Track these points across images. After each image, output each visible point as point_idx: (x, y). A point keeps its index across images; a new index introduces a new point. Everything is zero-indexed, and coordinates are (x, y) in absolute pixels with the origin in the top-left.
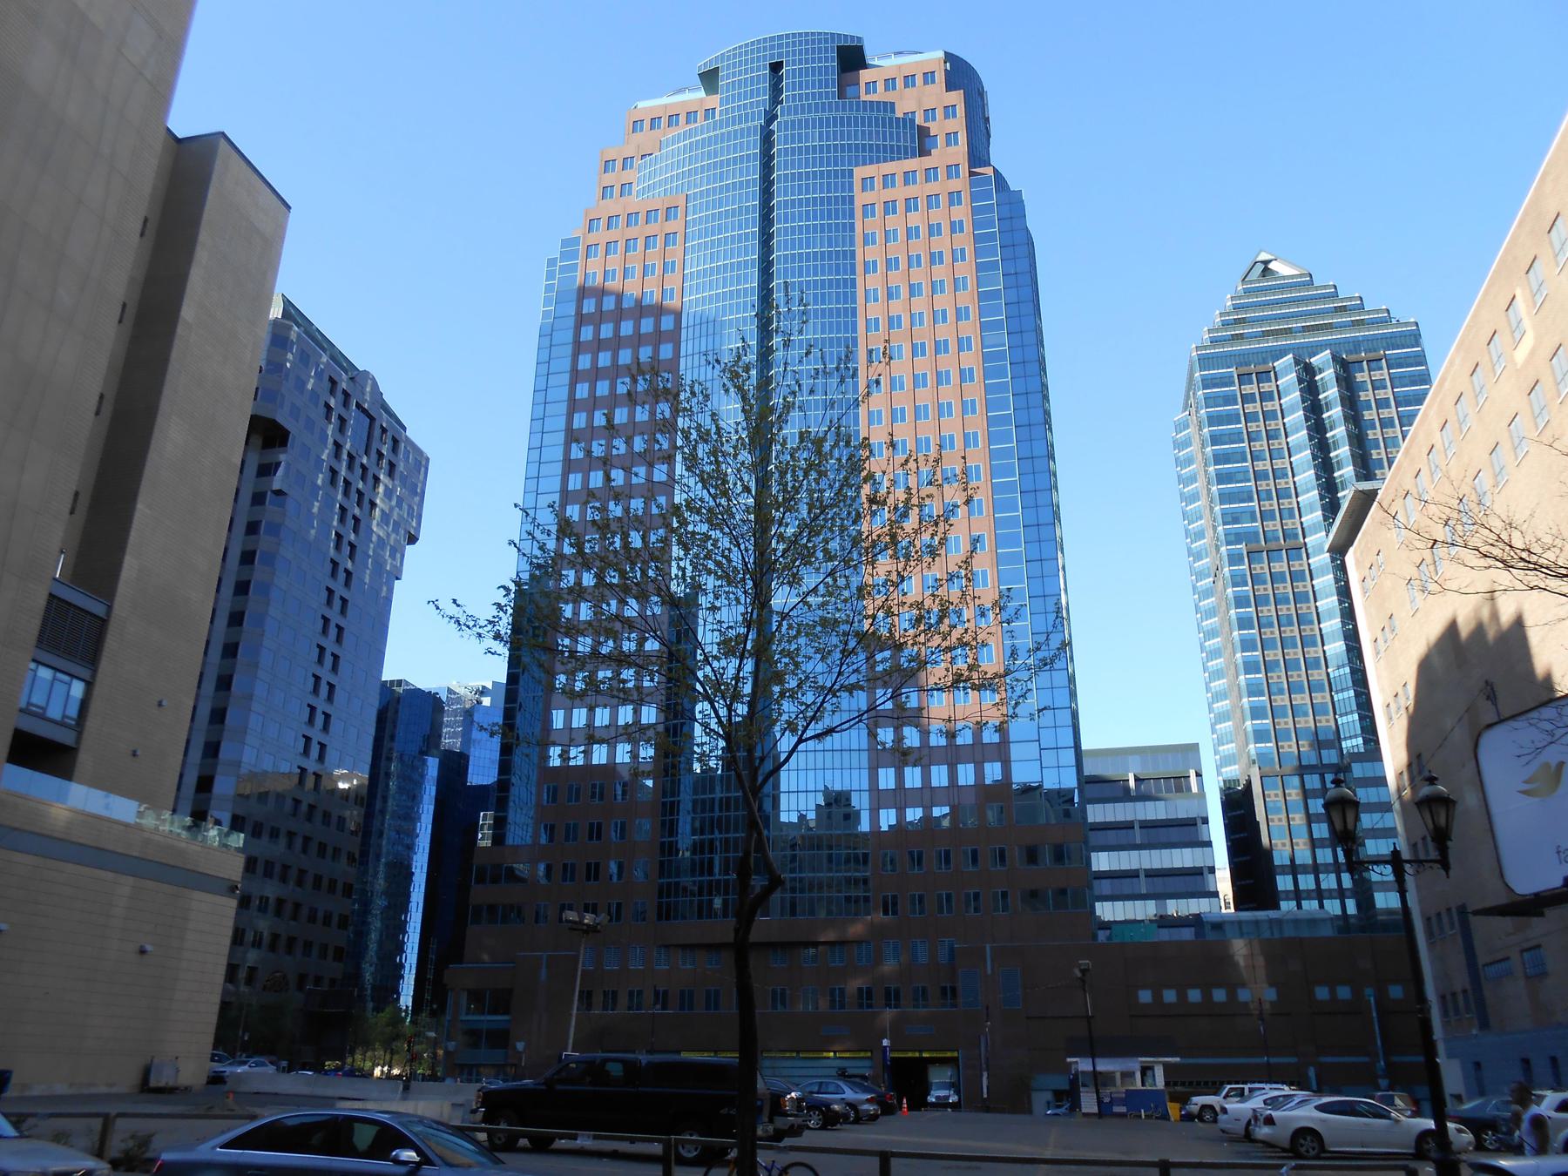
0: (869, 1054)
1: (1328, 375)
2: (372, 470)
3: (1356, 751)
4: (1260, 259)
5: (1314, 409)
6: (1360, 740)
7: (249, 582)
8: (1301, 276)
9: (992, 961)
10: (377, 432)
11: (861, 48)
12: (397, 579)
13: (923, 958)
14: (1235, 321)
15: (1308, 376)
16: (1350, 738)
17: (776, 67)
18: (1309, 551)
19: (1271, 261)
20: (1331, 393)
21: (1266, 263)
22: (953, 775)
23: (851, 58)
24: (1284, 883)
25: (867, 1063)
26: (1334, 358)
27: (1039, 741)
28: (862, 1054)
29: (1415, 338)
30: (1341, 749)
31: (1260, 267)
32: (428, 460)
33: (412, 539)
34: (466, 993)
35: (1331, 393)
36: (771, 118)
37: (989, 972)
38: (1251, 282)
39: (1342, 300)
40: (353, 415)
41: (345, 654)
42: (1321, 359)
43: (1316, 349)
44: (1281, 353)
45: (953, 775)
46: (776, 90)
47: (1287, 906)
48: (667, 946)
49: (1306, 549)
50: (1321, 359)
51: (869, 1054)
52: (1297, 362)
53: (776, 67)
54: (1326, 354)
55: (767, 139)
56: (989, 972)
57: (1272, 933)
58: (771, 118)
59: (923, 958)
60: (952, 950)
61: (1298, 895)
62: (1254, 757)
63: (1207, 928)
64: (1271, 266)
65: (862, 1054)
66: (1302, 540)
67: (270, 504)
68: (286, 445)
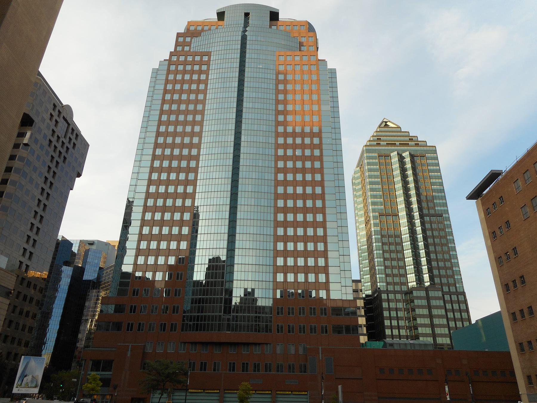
0: (270, 392)
1: (408, 160)
2: (67, 144)
3: (413, 286)
4: (384, 121)
5: (403, 170)
6: (415, 283)
7: (8, 180)
8: (398, 128)
9: (321, 354)
10: (70, 130)
11: (279, 13)
12: (72, 189)
13: (292, 350)
14: (377, 140)
15: (401, 159)
16: (412, 282)
17: (247, 15)
18: (400, 217)
19: (387, 122)
20: (409, 166)
21: (386, 122)
22: (306, 278)
23: (274, 16)
24: (388, 332)
25: (269, 396)
26: (410, 154)
27: (340, 266)
28: (267, 392)
29: (435, 152)
30: (408, 286)
31: (384, 124)
32: (89, 145)
33: (79, 175)
34: (91, 362)
35: (409, 166)
36: (245, 31)
37: (321, 359)
38: (382, 127)
39: (412, 137)
40: (61, 120)
41: (46, 216)
42: (406, 154)
43: (405, 151)
44: (393, 151)
45: (306, 278)
46: (246, 24)
47: (388, 340)
48: (185, 343)
49: (399, 216)
50: (406, 154)
51: (270, 392)
52: (398, 154)
53: (247, 15)
54: (408, 153)
55: (244, 39)
56: (321, 359)
57: (411, 347)
58: (245, 31)
59: (292, 350)
60: (304, 348)
61: (392, 336)
62: (379, 287)
63: (388, 345)
64: (388, 123)
65: (267, 392)
66: (397, 213)
67: (17, 160)
68: (32, 126)
